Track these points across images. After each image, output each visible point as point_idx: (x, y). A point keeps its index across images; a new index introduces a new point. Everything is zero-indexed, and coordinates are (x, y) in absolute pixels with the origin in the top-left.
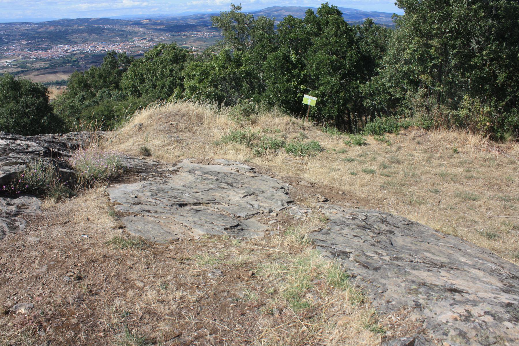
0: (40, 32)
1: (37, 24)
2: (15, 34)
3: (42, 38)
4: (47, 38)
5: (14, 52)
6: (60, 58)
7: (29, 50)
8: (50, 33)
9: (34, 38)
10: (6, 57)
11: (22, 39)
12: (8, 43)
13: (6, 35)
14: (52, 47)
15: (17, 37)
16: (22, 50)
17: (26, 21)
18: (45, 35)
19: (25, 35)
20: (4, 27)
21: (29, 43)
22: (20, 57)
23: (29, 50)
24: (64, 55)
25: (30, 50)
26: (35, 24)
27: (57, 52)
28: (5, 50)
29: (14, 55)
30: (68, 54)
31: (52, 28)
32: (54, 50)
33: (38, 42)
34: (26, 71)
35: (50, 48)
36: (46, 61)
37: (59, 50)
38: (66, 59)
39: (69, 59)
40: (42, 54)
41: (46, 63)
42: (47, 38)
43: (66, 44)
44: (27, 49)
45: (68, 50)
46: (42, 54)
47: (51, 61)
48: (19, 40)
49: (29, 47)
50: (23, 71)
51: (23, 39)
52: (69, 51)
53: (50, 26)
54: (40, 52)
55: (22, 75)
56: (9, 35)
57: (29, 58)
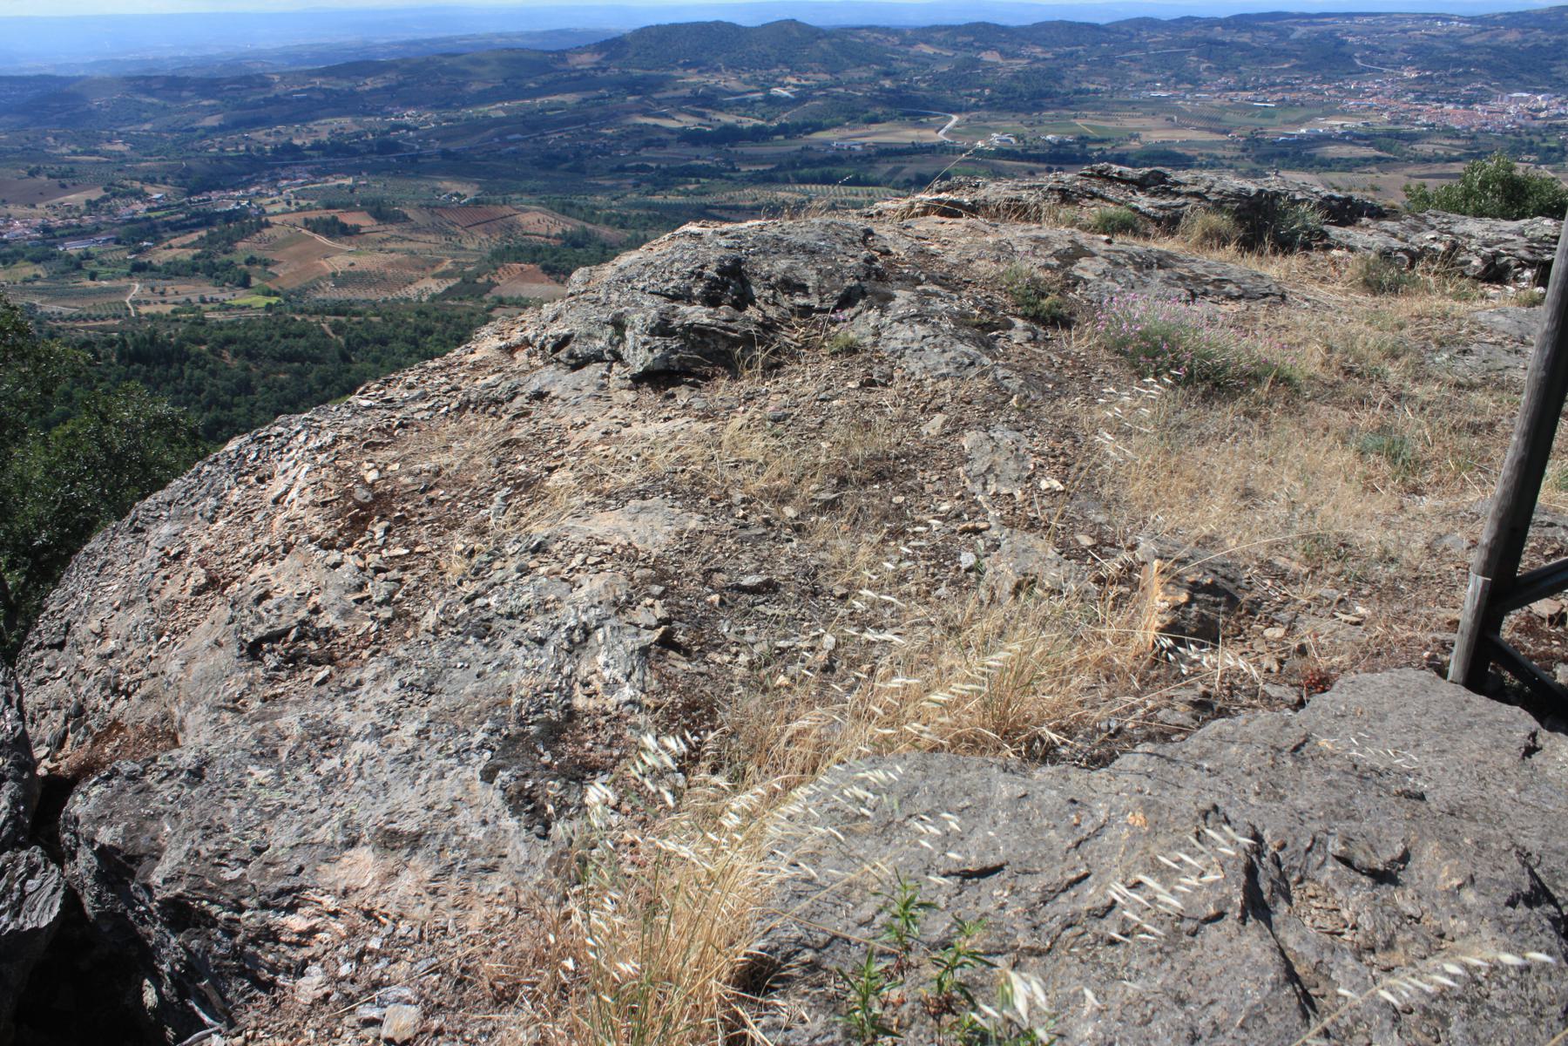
0: (1469, 47)
1: (1472, 20)
2: (1393, 46)
3: (1470, 64)
4: (1487, 65)
5: (1373, 101)
6: (1505, 132)
7: (1417, 99)
8: (1500, 51)
9: (1445, 63)
10: (1344, 113)
11: (1408, 64)
12: (1363, 71)
13: (1367, 47)
14: (1490, 97)
15: (1396, 57)
16: (1397, 96)
17: (1449, 12)
18: (1481, 58)
19: (1422, 54)
20: (1369, 24)
21: (1427, 77)
22: (1386, 116)
23: (1417, 99)
24: (1521, 127)
25: (1421, 97)
26: (1462, 19)
27: (1503, 112)
28: (1350, 91)
29: (1370, 107)
30: (1537, 123)
31: (1511, 37)
32: (1495, 105)
33: (1454, 76)
34: (1387, 160)
35: (1483, 97)
36: (1458, 137)
37: (1512, 109)
38: (1526, 139)
39: (1537, 139)
40: (1453, 114)
41: (1457, 142)
42: (1487, 65)
43: (1543, 91)
44: (1412, 96)
45: (1541, 110)
46: (1453, 114)
47: (1473, 138)
48: (1398, 66)
49: (1421, 88)
50: (1378, 159)
51: (1412, 63)
52: (1542, 115)
53: (1508, 28)
54: (1451, 107)
55: (1374, 169)
56: (1374, 49)
57: (1411, 122)
